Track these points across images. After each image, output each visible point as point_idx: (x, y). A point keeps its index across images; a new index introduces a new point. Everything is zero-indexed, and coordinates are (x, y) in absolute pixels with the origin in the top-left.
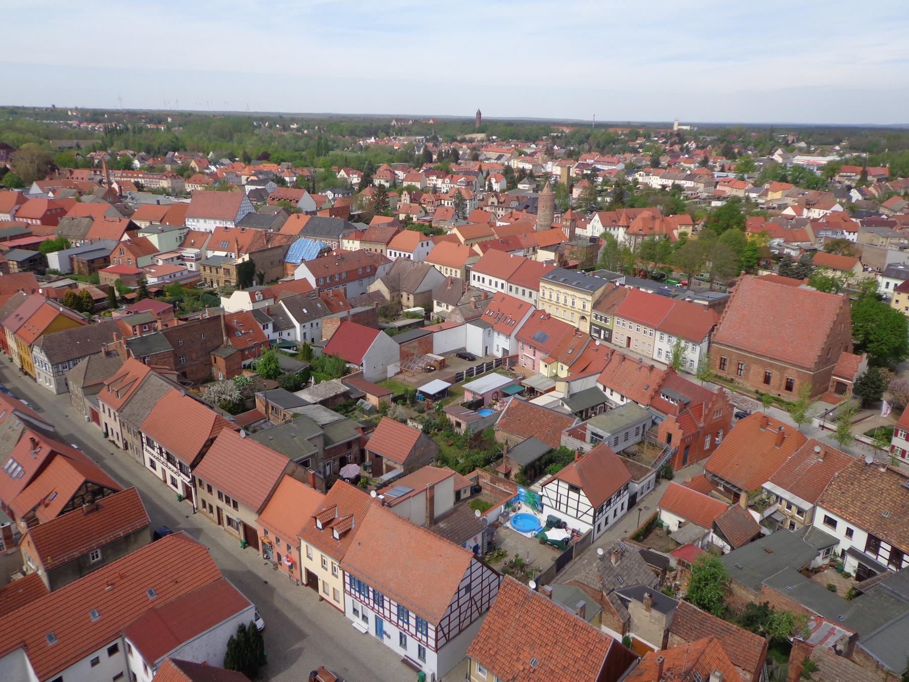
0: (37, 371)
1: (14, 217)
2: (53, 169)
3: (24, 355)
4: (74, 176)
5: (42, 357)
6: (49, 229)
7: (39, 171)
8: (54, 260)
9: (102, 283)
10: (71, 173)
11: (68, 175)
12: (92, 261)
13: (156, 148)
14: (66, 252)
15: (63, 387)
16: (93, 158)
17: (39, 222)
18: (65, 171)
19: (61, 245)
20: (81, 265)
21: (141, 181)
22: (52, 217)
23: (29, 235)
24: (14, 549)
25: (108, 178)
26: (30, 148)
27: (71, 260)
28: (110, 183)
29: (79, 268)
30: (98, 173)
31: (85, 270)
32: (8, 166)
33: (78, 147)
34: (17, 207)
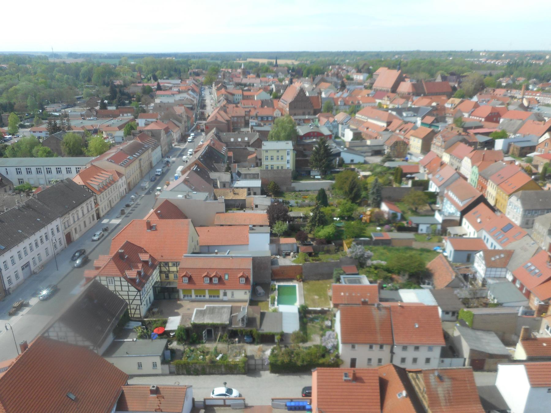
0: (507, 210)
1: (470, 115)
2: (483, 89)
3: (500, 199)
4: (495, 93)
5: (519, 204)
6: (493, 124)
7: (475, 89)
8: (499, 144)
9: (534, 163)
10: (494, 91)
11: (492, 92)
12: (523, 148)
13: (542, 76)
14: (508, 141)
15: (528, 224)
16: (501, 82)
17: (483, 120)
18: (490, 90)
19: (503, 135)
20: (515, 150)
21: (538, 98)
22: (493, 117)
23: (481, 127)
24: (539, 318)
25: (524, 94)
26: (473, 76)
27: (510, 145)
28: (522, 98)
29: (513, 151)
30: (509, 91)
31: (517, 153)
32: (456, 85)
33: (491, 75)
34: (473, 110)
